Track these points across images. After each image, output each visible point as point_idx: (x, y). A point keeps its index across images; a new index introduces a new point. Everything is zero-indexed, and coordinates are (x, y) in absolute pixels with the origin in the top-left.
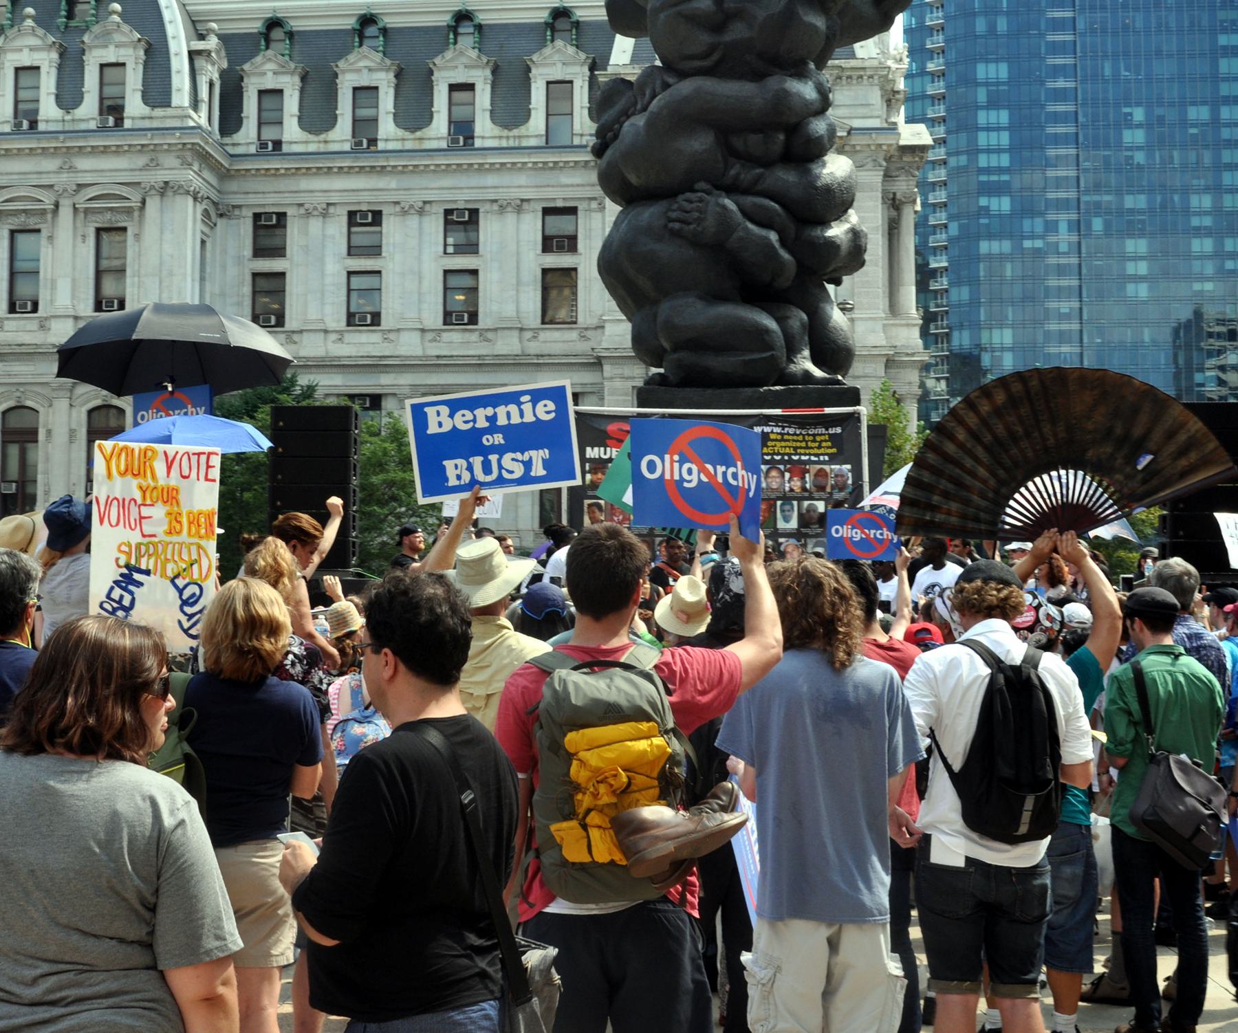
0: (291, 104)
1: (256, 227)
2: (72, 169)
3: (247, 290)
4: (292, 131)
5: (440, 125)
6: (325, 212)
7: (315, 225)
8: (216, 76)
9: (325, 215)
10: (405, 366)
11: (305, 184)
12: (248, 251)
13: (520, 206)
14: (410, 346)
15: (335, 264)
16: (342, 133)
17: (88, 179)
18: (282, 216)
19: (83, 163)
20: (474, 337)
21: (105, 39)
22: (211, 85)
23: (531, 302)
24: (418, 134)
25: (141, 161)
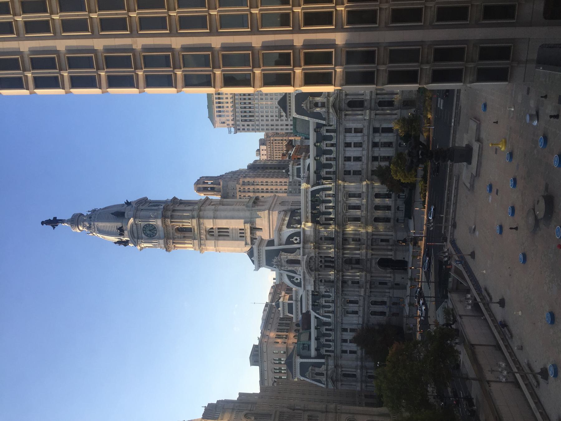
0: (328, 170)
1: (346, 175)
2: (340, 201)
3: (355, 176)
4: (332, 170)
5: (332, 148)
6: (344, 165)
7: (346, 166)
8: (325, 181)
9: (345, 165)
10: (368, 153)
11: (340, 168)
12: (350, 176)
13: (345, 136)
14: (365, 152)
15: (352, 163)
16: (333, 163)
17: (342, 199)
18: (345, 171)
19: (340, 199)
20: (364, 143)
21: (322, 197)
22: (326, 181)
23: (359, 134)
24: (333, 151)
25: (339, 191)
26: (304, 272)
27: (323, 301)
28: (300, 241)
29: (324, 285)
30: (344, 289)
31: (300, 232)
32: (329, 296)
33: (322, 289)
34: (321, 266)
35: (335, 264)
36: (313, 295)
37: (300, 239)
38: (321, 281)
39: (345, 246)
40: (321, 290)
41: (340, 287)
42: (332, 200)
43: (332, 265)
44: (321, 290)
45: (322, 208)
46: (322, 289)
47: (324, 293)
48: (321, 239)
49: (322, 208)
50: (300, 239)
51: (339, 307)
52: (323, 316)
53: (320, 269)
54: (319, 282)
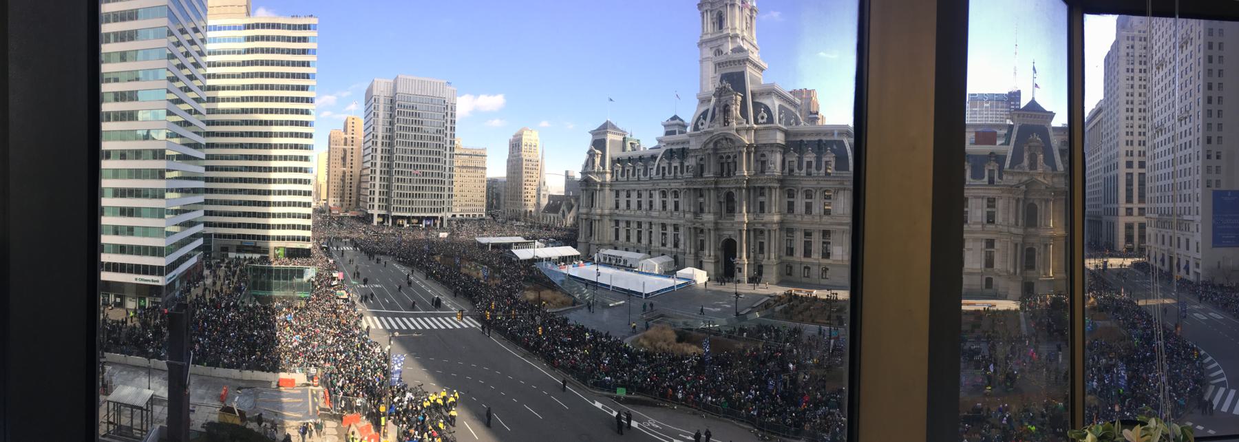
26: (712, 132)
27: (676, 163)
28: (761, 123)
29: (697, 164)
30: (692, 191)
31: (773, 123)
32: (682, 172)
33: (691, 162)
34: (722, 157)
35: (725, 177)
36: (683, 149)
37: (764, 123)
38: (701, 159)
39: (752, 191)
40: (690, 159)
41: (695, 187)
42: (821, 172)
43: (724, 173)
44: (690, 159)
45: (810, 157)
46: (691, 162)
47: (686, 164)
48: (763, 155)
49: (810, 157)
50: (764, 123)
51: (669, 185)
52: (659, 165)
53: (719, 155)
54: (700, 157)
